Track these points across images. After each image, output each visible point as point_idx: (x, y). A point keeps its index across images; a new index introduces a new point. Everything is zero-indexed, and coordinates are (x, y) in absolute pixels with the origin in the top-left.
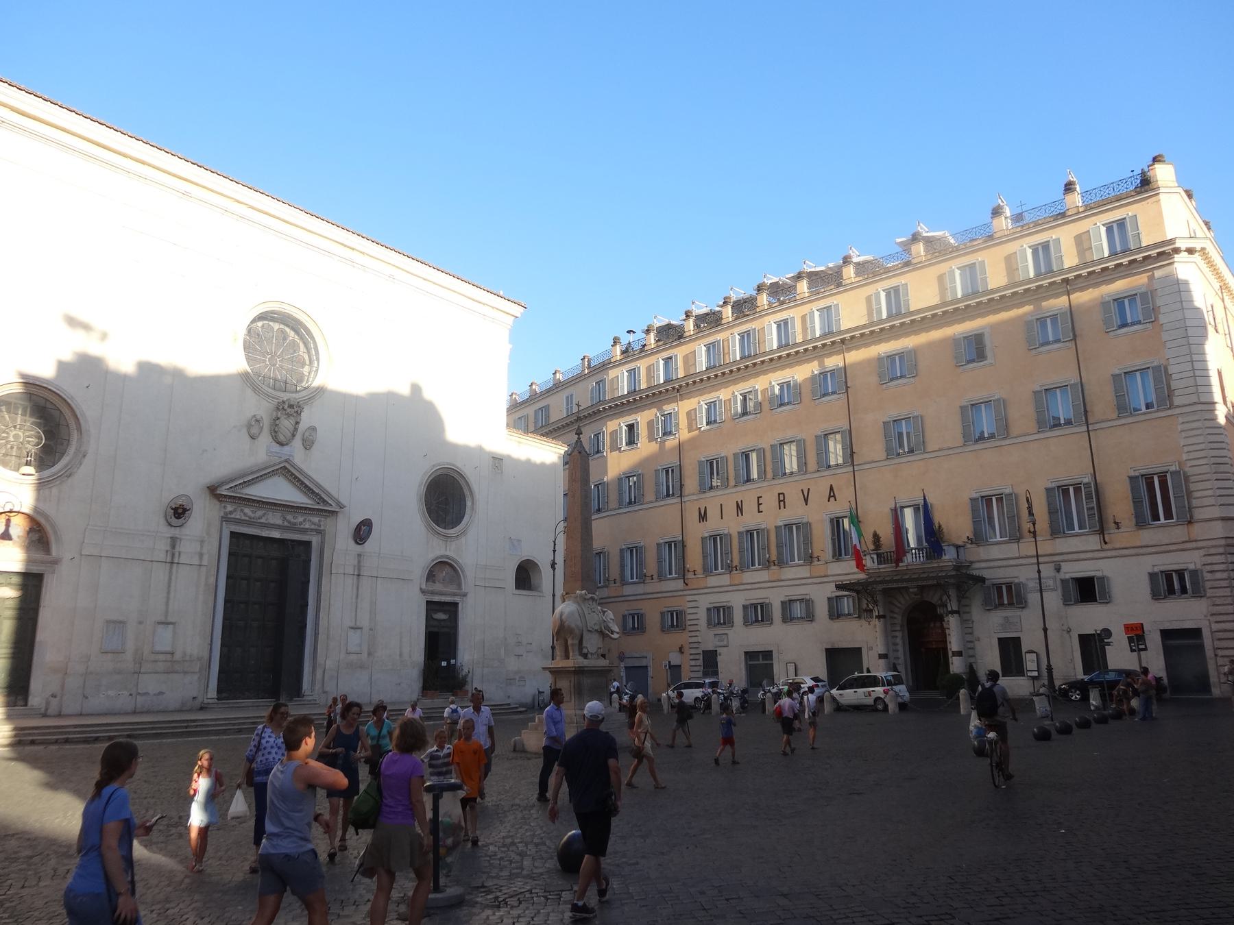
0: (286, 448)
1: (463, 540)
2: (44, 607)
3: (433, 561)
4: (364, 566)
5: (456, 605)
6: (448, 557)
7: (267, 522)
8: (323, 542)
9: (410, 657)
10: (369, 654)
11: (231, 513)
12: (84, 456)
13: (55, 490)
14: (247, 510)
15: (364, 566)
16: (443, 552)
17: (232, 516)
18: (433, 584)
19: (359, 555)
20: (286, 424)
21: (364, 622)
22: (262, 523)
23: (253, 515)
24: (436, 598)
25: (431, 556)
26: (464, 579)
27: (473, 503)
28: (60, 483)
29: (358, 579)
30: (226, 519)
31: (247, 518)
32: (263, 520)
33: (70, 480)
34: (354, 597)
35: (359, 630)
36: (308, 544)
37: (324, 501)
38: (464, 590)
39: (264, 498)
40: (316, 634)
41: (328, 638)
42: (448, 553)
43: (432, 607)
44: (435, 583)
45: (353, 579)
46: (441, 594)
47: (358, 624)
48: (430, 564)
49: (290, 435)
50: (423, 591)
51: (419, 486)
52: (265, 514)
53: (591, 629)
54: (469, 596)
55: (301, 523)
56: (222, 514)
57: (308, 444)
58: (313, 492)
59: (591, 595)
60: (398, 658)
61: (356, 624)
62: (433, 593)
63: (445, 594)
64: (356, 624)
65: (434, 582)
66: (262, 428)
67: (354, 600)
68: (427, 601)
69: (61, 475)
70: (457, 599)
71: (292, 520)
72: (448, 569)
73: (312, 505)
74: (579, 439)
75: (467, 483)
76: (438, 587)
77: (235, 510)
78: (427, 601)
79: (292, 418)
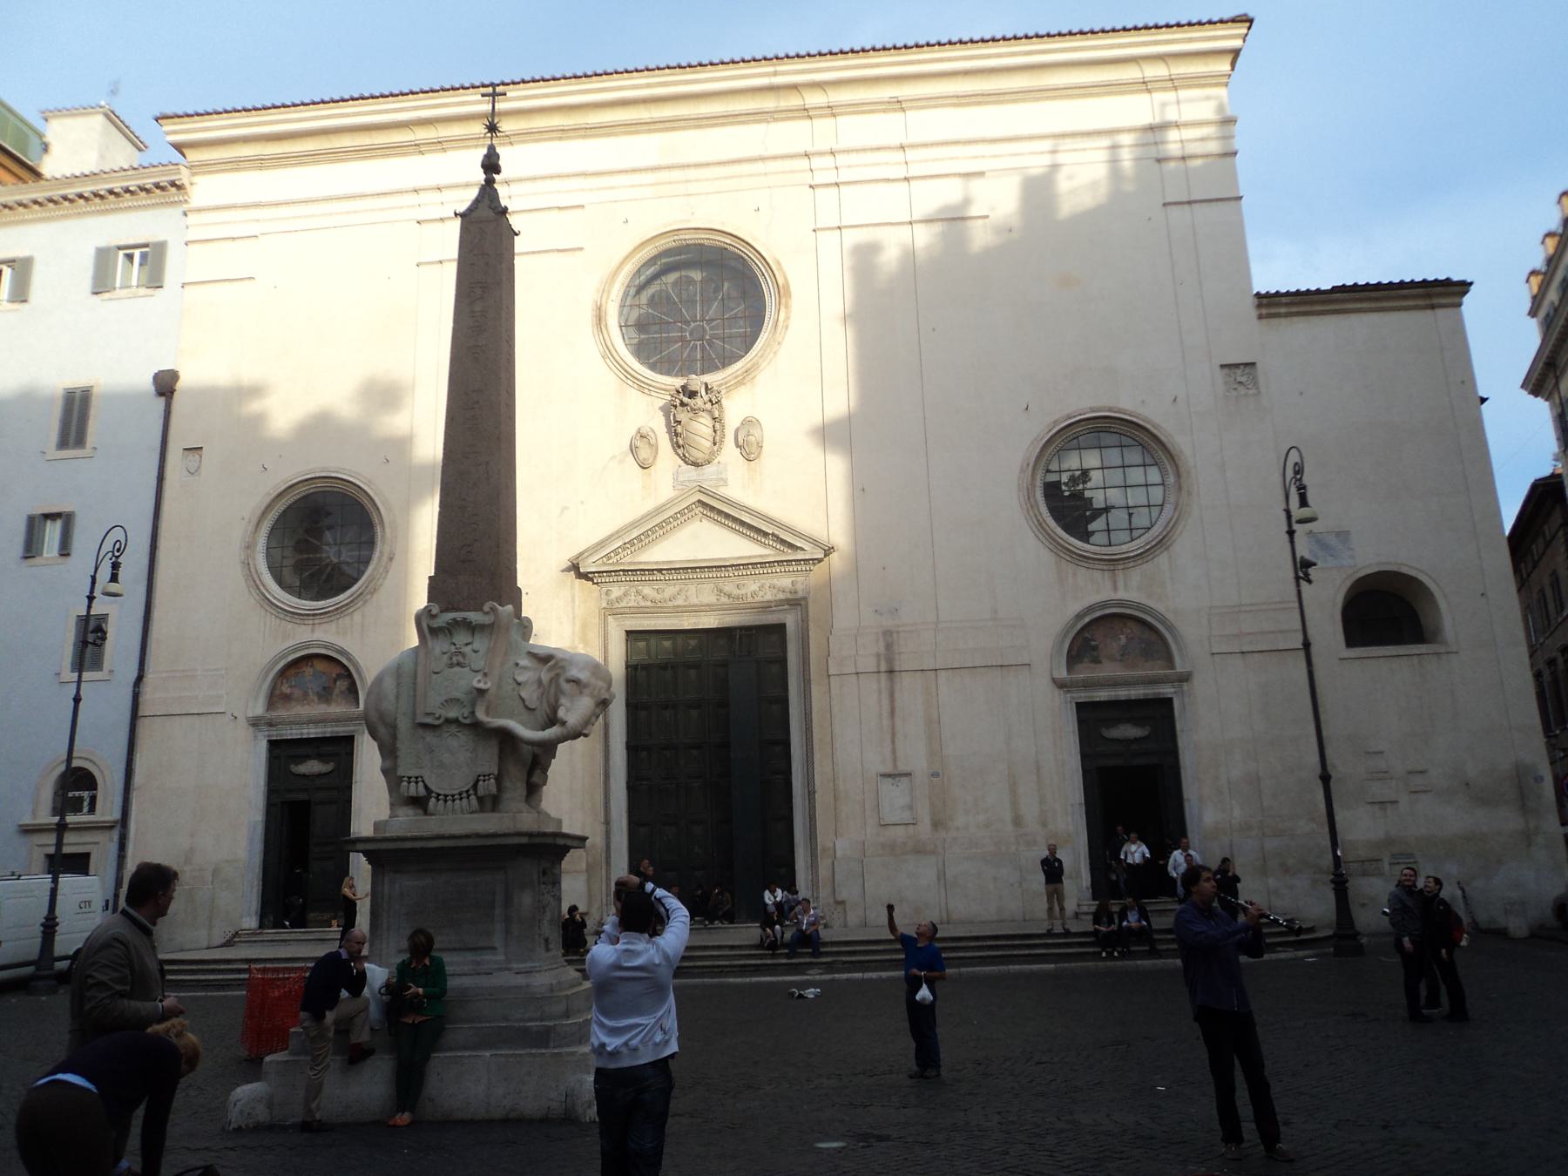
0: (708, 469)
1: (1162, 560)
2: (356, 782)
3: (1079, 616)
4: (900, 653)
5: (1167, 703)
6: (1121, 603)
7: (686, 604)
8: (805, 620)
9: (1044, 824)
10: (937, 824)
11: (618, 600)
12: (391, 559)
13: (357, 617)
14: (647, 590)
15: (900, 653)
16: (1106, 594)
17: (623, 604)
18: (1093, 665)
19: (888, 633)
20: (701, 427)
21: (915, 757)
22: (678, 606)
23: (658, 597)
24: (1103, 695)
25: (1076, 607)
26: (1177, 642)
27: (1178, 475)
28: (363, 604)
29: (892, 681)
30: (611, 611)
31: (649, 604)
32: (680, 602)
33: (375, 596)
34: (885, 713)
35: (905, 780)
36: (780, 628)
37: (791, 546)
38: (1180, 667)
39: (664, 562)
40: (811, 794)
41: (835, 799)
42: (1121, 595)
43: (1091, 717)
44: (1100, 662)
45: (879, 681)
46: (1114, 683)
47: (902, 767)
48: (1074, 625)
49: (708, 444)
50: (1060, 685)
51: (1022, 471)
52: (681, 590)
53: (429, 720)
54: (1197, 680)
55: (754, 594)
56: (604, 605)
57: (749, 450)
58: (766, 534)
59: (450, 616)
60: (1010, 827)
61: (895, 766)
62: (1087, 685)
63: (1126, 683)
64: (895, 766)
65: (1096, 661)
66: (654, 448)
67: (886, 722)
68: (1077, 703)
69: (361, 594)
70: (1166, 690)
71: (736, 592)
72: (1133, 628)
73: (761, 556)
74: (490, 182)
75: (1155, 437)
76: (1108, 670)
77: (625, 594)
78: (1077, 703)
79: (703, 414)
